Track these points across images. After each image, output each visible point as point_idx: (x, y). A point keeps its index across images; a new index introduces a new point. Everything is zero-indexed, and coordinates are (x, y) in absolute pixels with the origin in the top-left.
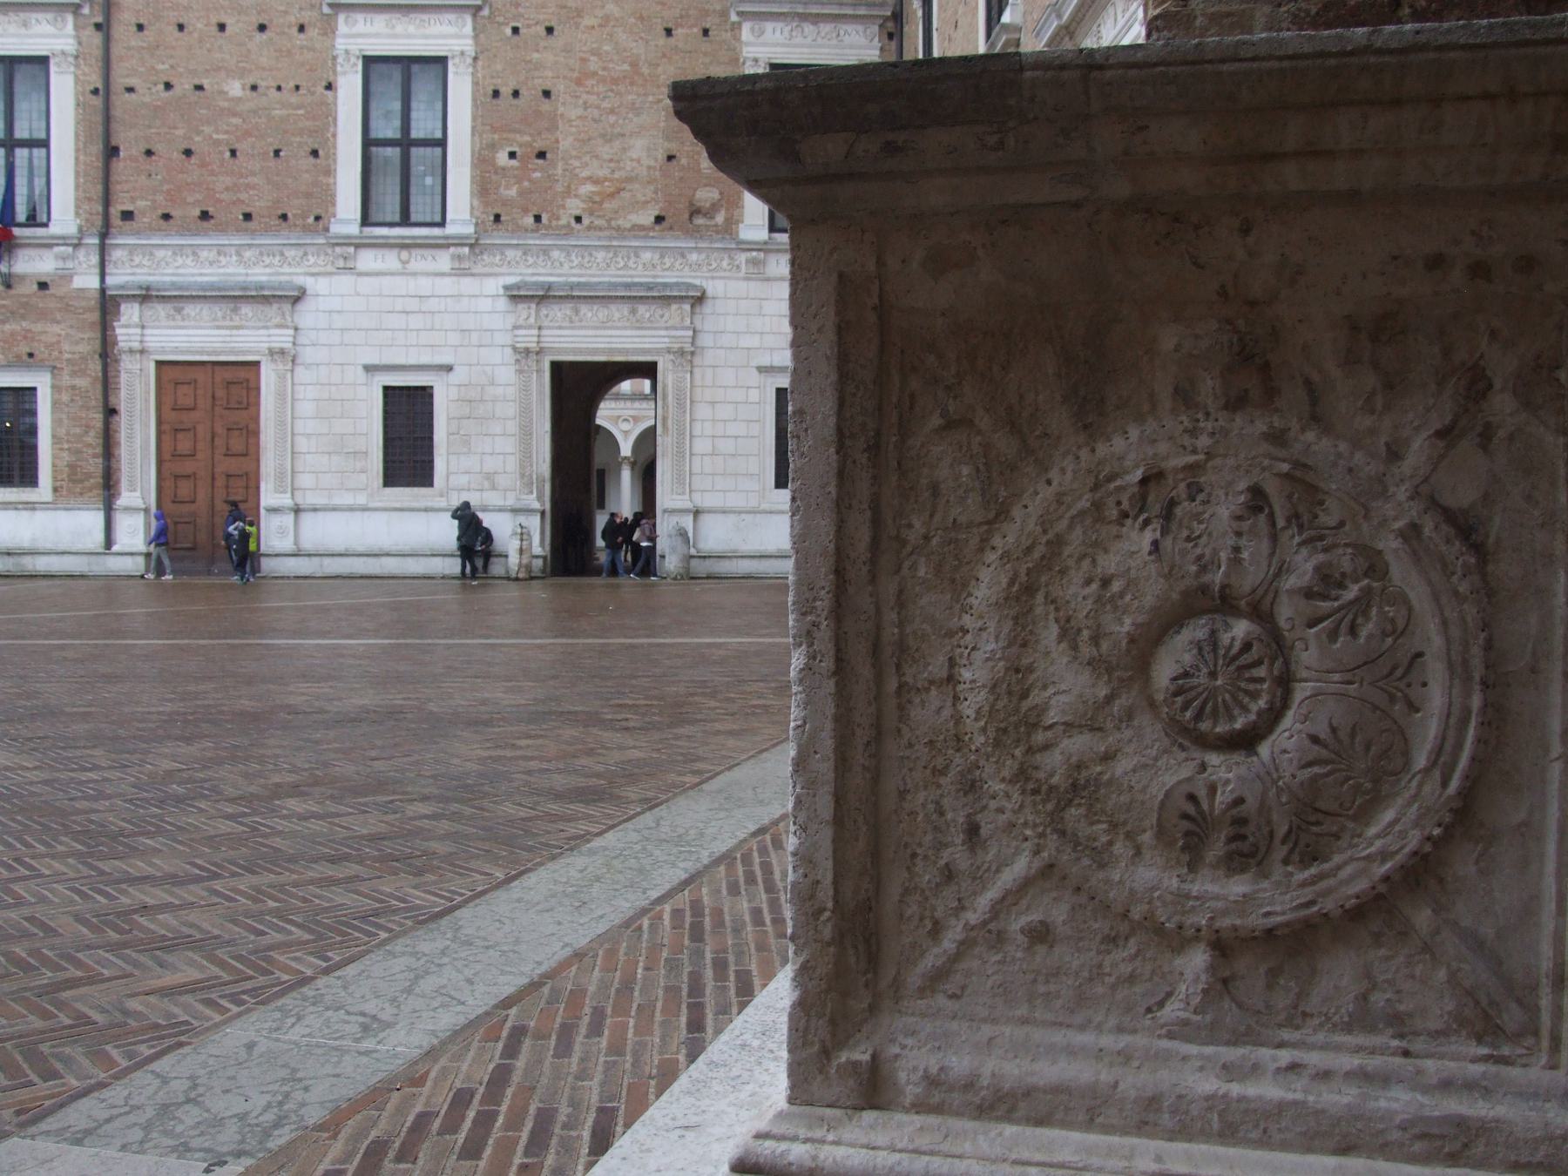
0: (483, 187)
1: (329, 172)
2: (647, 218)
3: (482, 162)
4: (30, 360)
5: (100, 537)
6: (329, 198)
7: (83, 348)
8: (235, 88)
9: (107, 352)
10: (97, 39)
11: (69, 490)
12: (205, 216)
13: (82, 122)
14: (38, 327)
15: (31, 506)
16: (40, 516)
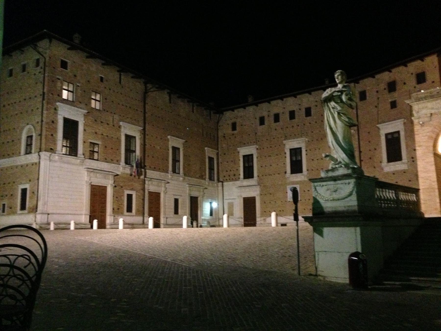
0: (184, 169)
1: (168, 163)
2: (197, 176)
3: (184, 165)
4: (132, 189)
5: (141, 222)
6: (168, 167)
7: (140, 188)
8: (158, 148)
9: (144, 190)
10: (142, 136)
11: (138, 214)
12: (155, 168)
13: (141, 149)
14: (134, 184)
15: (133, 216)
16: (134, 218)
